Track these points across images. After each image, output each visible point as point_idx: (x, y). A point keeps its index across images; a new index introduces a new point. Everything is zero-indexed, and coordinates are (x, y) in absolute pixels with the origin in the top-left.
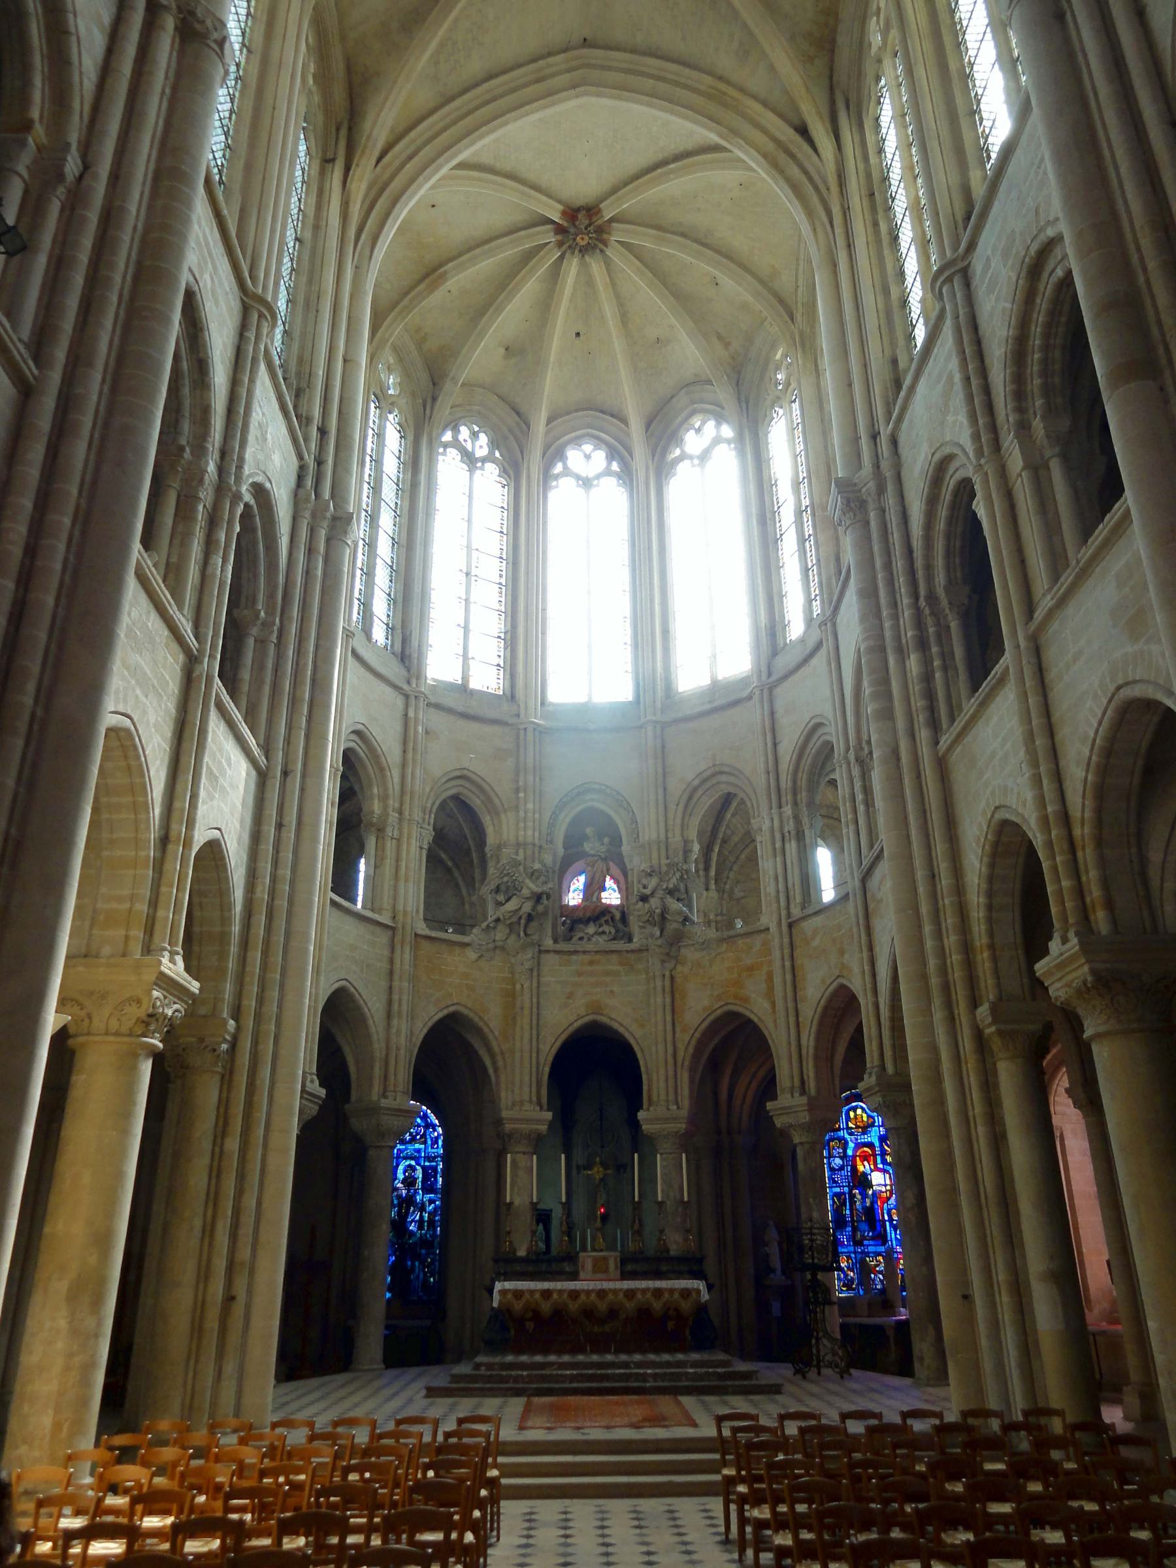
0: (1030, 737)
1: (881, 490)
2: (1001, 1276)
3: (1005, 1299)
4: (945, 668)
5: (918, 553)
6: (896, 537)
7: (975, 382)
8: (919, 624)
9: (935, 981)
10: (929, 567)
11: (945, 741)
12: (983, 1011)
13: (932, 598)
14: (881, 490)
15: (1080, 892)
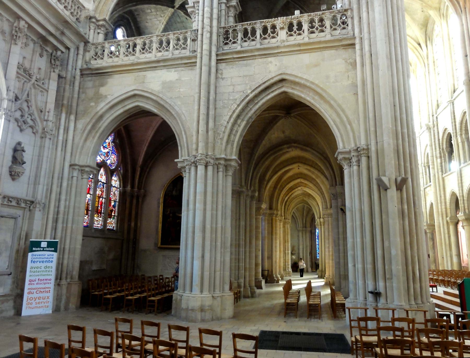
0: (459, 184)
1: (434, 127)
2: (449, 255)
3: (449, 258)
4: (444, 162)
5: (441, 140)
6: (436, 137)
7: (453, 124)
8: (440, 153)
9: (440, 213)
10: (442, 143)
11: (444, 175)
12: (448, 218)
13: (443, 149)
14: (434, 127)
15: (464, 207)
